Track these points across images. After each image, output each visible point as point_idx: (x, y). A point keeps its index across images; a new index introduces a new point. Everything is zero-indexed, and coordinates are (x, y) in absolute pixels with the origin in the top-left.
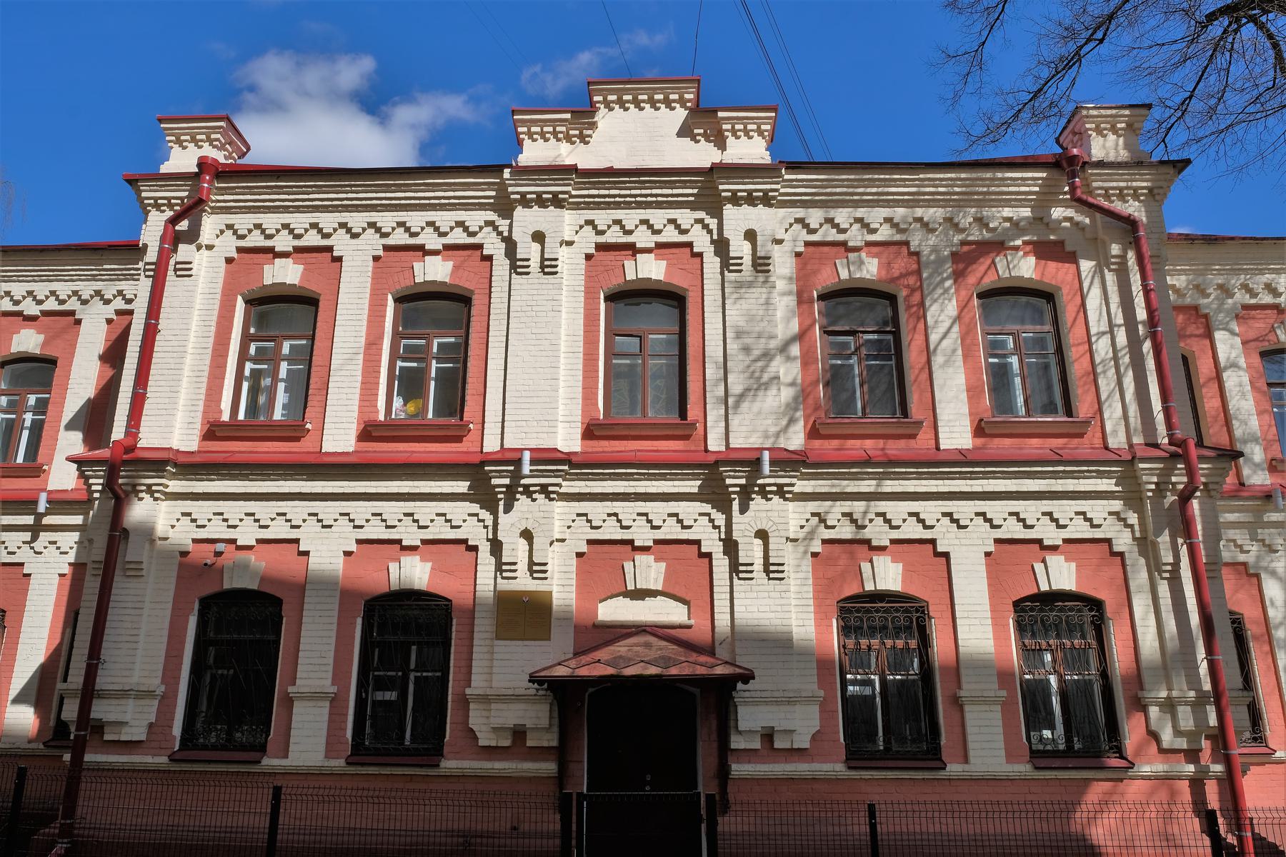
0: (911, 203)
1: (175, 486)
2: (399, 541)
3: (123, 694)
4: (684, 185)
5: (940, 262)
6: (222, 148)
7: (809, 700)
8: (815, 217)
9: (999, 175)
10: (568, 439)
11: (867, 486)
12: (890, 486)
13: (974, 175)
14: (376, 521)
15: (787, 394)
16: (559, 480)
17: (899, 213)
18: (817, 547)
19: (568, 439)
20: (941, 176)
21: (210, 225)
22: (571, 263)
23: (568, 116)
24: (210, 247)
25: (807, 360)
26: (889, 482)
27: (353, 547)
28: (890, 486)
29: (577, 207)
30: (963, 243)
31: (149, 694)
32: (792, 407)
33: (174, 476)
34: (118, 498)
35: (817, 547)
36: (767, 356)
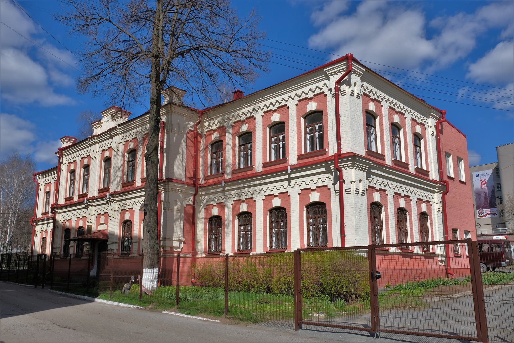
0: (136, 128)
1: (61, 211)
2: (310, 188)
3: (56, 248)
4: (106, 135)
5: (140, 141)
6: (67, 142)
7: (116, 243)
8: (124, 135)
9: (145, 117)
10: (96, 194)
11: (124, 198)
12: (127, 197)
13: (142, 118)
14: (319, 181)
15: (119, 179)
16: (91, 203)
17: (135, 130)
18: (120, 211)
19: (96, 194)
20: (137, 120)
21: (65, 159)
22: (98, 155)
23: (97, 122)
24: (65, 164)
25: (123, 170)
26: (126, 196)
27: (300, 192)
28: (127, 197)
29: (98, 143)
30: (145, 134)
31: (59, 248)
32: (120, 182)
33: (60, 209)
34: (54, 214)
35: (120, 211)
36: (116, 172)
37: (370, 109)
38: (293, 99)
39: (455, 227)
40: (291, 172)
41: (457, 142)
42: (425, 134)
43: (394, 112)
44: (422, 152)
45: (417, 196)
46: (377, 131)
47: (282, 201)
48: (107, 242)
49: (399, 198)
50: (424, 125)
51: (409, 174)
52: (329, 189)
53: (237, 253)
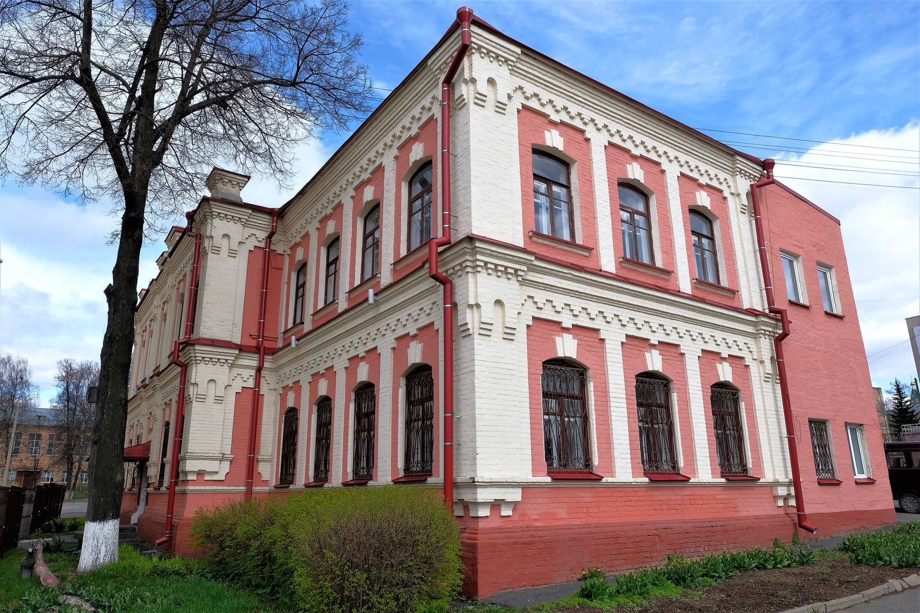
37: (548, 145)
38: (391, 146)
39: (818, 415)
40: (375, 300)
41: (815, 231)
42: (725, 210)
43: (627, 156)
44: (717, 248)
45: (700, 345)
46: (573, 194)
47: (370, 368)
48: (148, 463)
49: (643, 350)
50: (721, 191)
51: (678, 293)
52: (437, 330)
53: (313, 484)
